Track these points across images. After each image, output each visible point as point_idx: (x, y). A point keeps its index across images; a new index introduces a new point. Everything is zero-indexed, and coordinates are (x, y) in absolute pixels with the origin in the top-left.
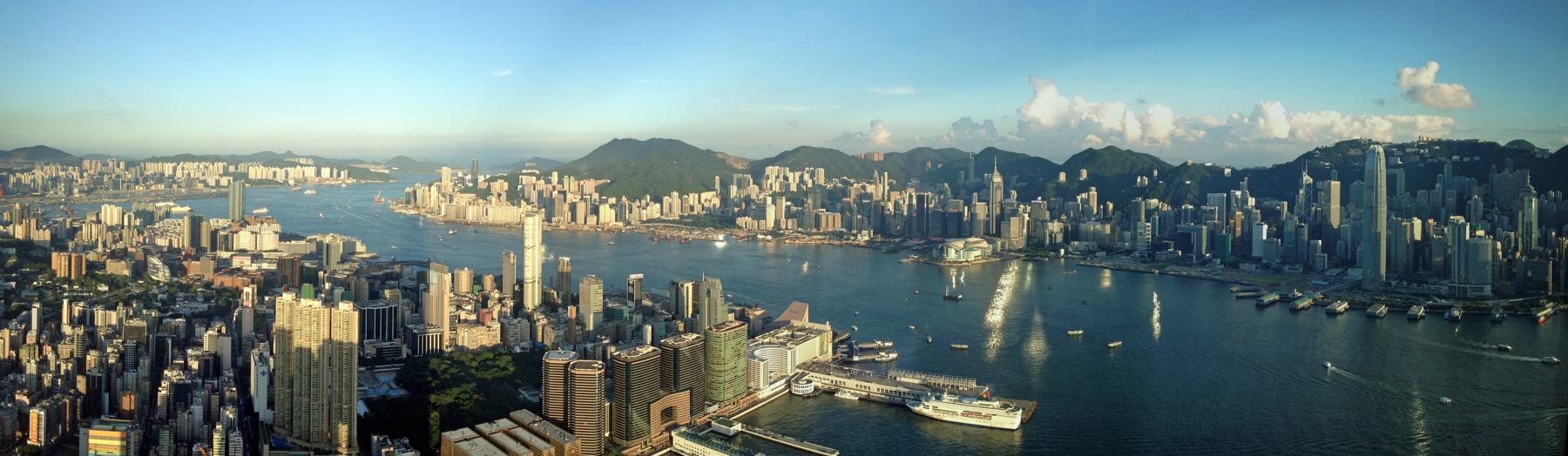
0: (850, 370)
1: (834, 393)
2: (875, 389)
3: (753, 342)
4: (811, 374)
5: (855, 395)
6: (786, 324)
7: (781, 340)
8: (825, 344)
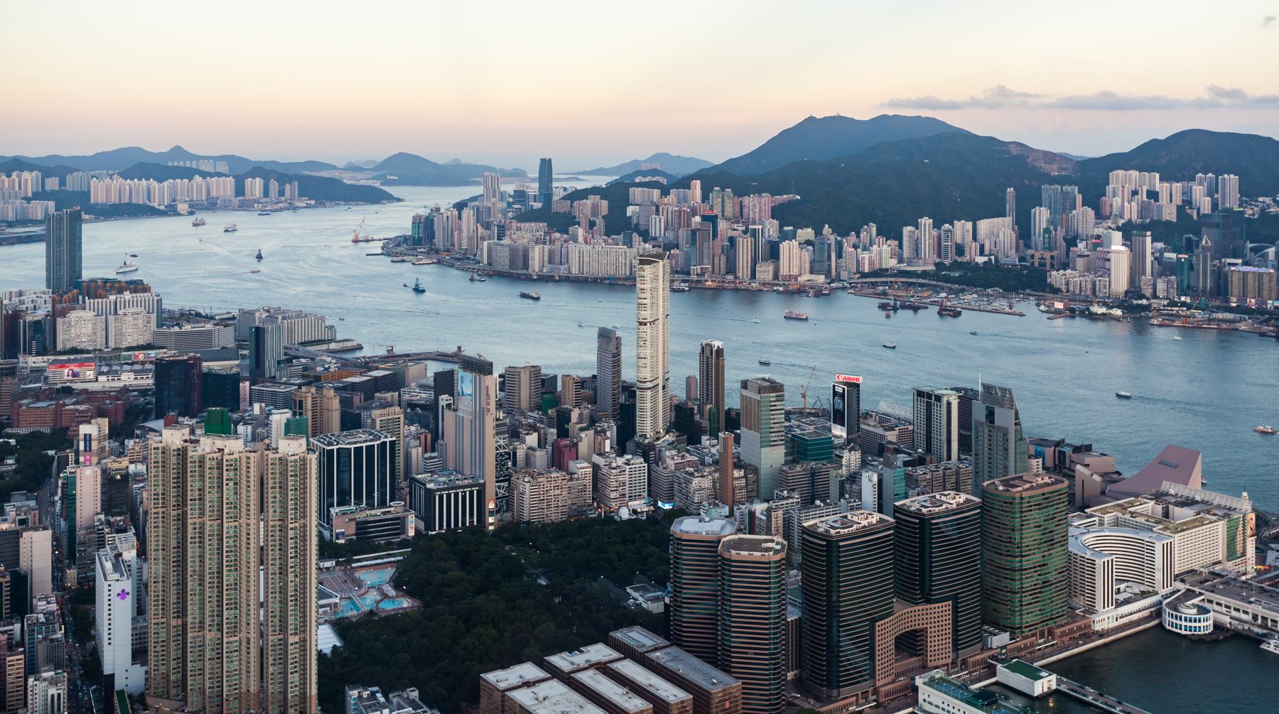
1: (1262, 642)
4: (1209, 595)
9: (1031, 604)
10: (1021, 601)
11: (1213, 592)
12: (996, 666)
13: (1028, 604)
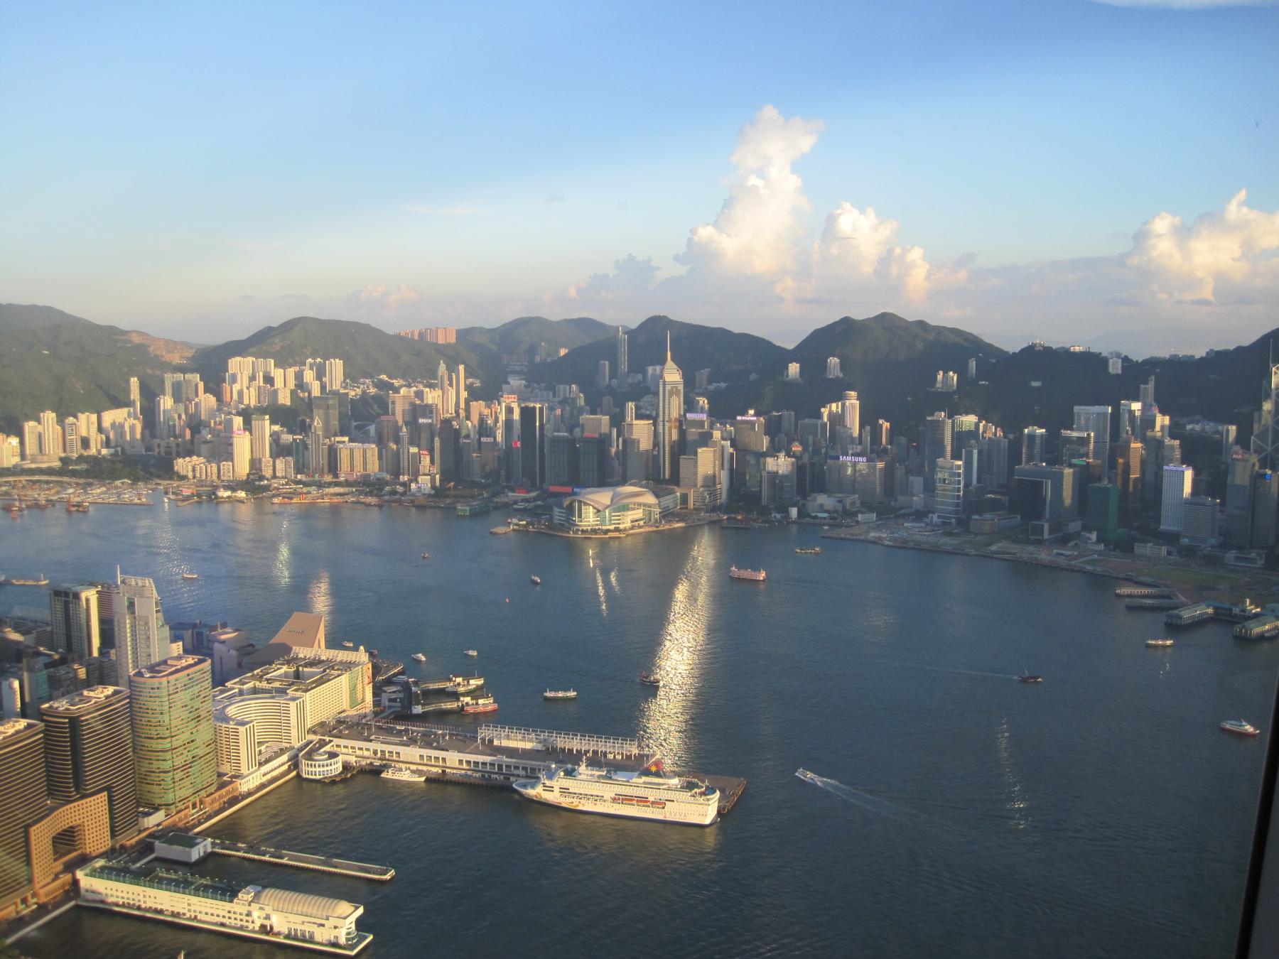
0: (406, 731)
1: (381, 772)
2: (455, 761)
3: (222, 692)
4: (336, 741)
5: (420, 773)
6: (281, 653)
7: (277, 685)
8: (359, 687)
9: (183, 779)
10: (173, 778)
11: (340, 737)
12: (152, 844)
13: (180, 780)
